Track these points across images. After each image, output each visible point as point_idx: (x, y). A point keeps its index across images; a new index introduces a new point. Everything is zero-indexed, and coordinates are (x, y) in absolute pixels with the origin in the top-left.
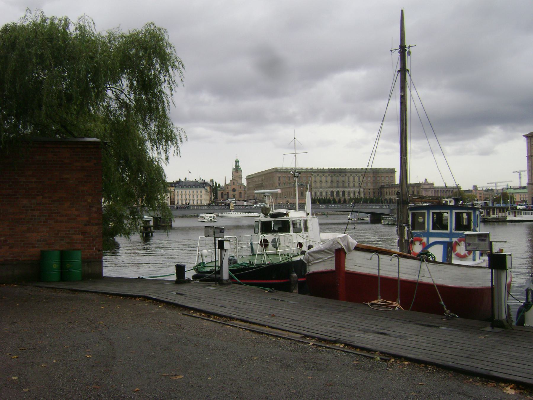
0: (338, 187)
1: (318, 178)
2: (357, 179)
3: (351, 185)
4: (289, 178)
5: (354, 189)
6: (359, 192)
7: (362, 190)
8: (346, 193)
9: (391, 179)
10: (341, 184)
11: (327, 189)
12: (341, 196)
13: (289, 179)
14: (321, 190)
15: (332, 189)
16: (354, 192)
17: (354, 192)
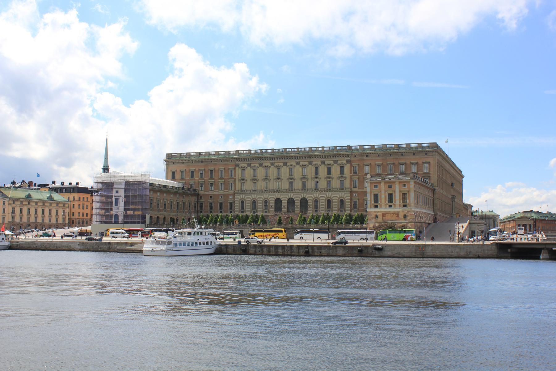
0: (291, 189)
1: (249, 172)
2: (336, 171)
3: (323, 184)
4: (192, 172)
5: (329, 194)
6: (342, 202)
7: (346, 196)
8: (310, 203)
9: (426, 169)
10: (298, 185)
11: (266, 196)
12: (297, 209)
13: (192, 176)
14: (254, 196)
15: (277, 196)
16: (329, 202)
17: (329, 202)
